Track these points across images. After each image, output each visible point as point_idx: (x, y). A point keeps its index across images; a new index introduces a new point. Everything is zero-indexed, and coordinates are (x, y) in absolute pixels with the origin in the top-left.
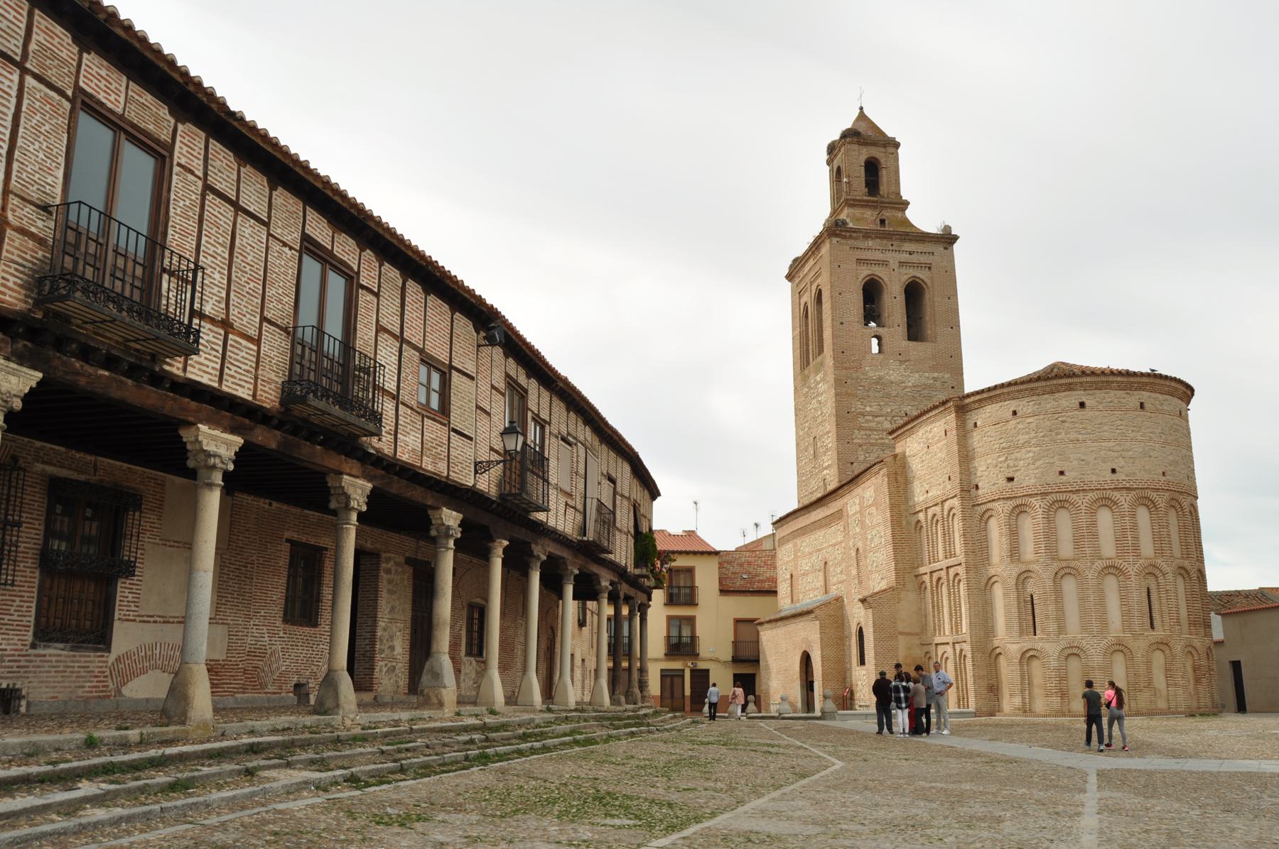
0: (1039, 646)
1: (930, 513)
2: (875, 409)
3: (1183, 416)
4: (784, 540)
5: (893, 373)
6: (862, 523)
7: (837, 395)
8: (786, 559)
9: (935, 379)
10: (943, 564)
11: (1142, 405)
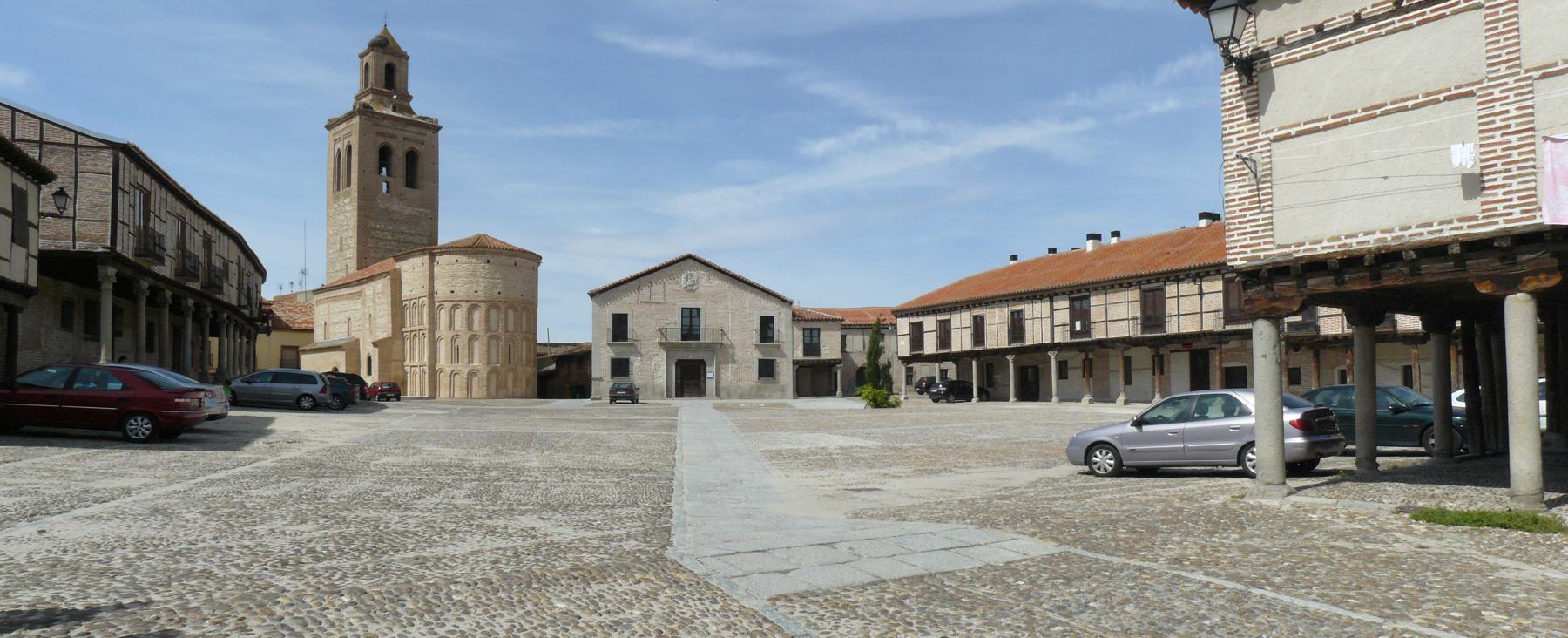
0: (459, 369)
1: (412, 302)
2: (383, 226)
3: (535, 270)
4: (319, 302)
5: (396, 206)
6: (374, 301)
7: (359, 215)
8: (321, 313)
9: (421, 212)
10: (418, 328)
11: (515, 264)
